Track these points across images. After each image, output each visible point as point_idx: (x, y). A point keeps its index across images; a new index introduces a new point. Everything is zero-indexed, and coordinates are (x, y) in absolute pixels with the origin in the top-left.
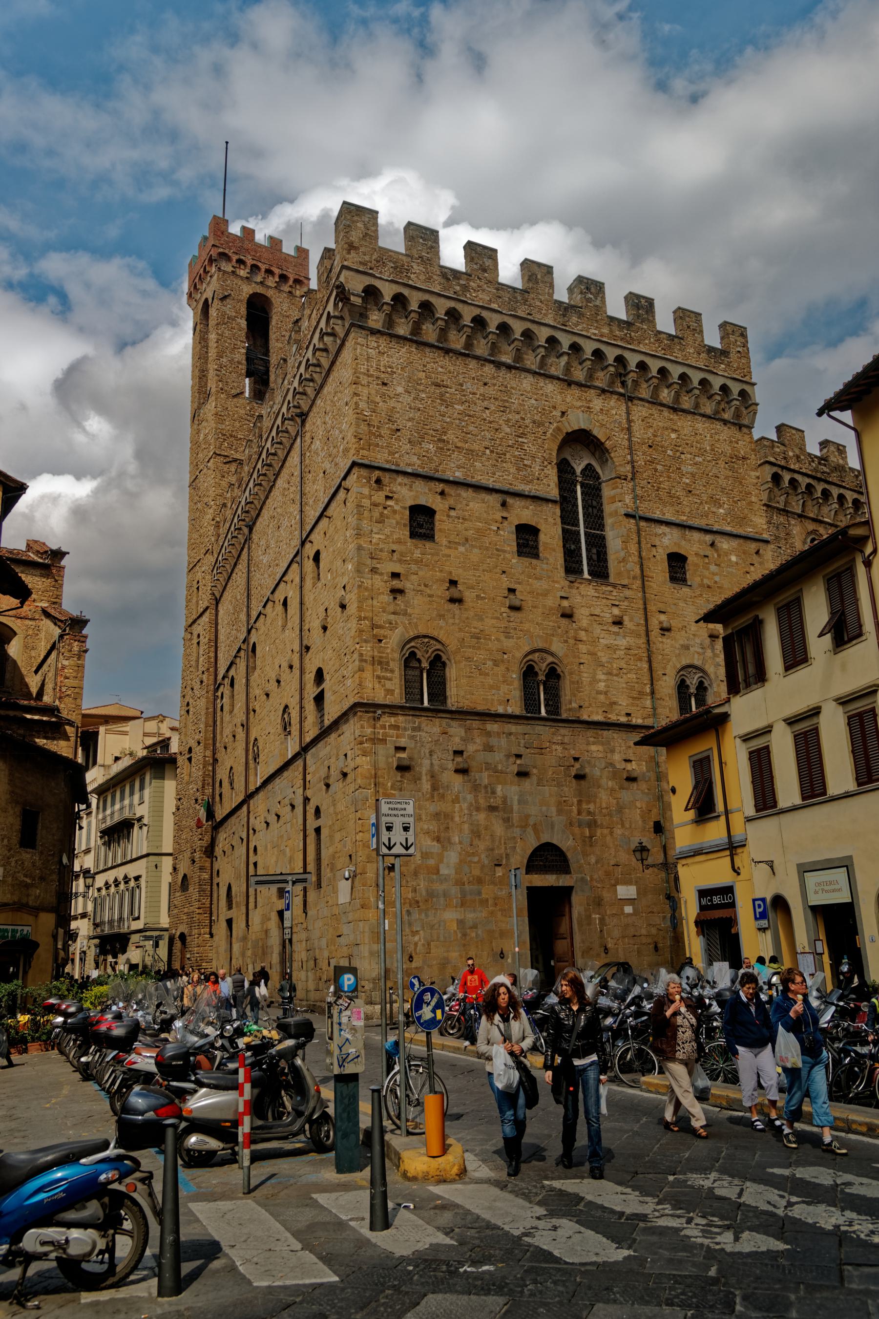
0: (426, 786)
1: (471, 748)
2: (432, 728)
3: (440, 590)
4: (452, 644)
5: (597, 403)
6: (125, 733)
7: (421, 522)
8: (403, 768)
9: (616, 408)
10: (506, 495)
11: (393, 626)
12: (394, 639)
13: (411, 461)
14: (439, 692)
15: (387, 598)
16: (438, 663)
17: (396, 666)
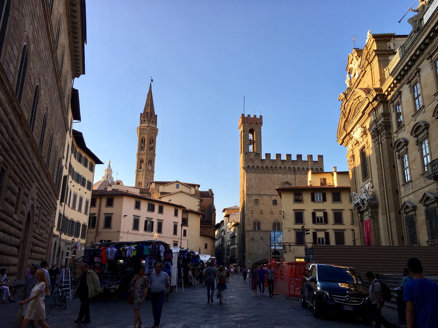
0: (256, 242)
1: (263, 236)
2: (257, 233)
3: (259, 212)
4: (261, 221)
5: (289, 176)
6: (235, 215)
7: (257, 201)
8: (252, 239)
9: (293, 176)
10: (270, 196)
11: (251, 218)
12: (251, 220)
13: (255, 192)
14: (259, 228)
15: (250, 214)
16: (259, 224)
17: (252, 225)
